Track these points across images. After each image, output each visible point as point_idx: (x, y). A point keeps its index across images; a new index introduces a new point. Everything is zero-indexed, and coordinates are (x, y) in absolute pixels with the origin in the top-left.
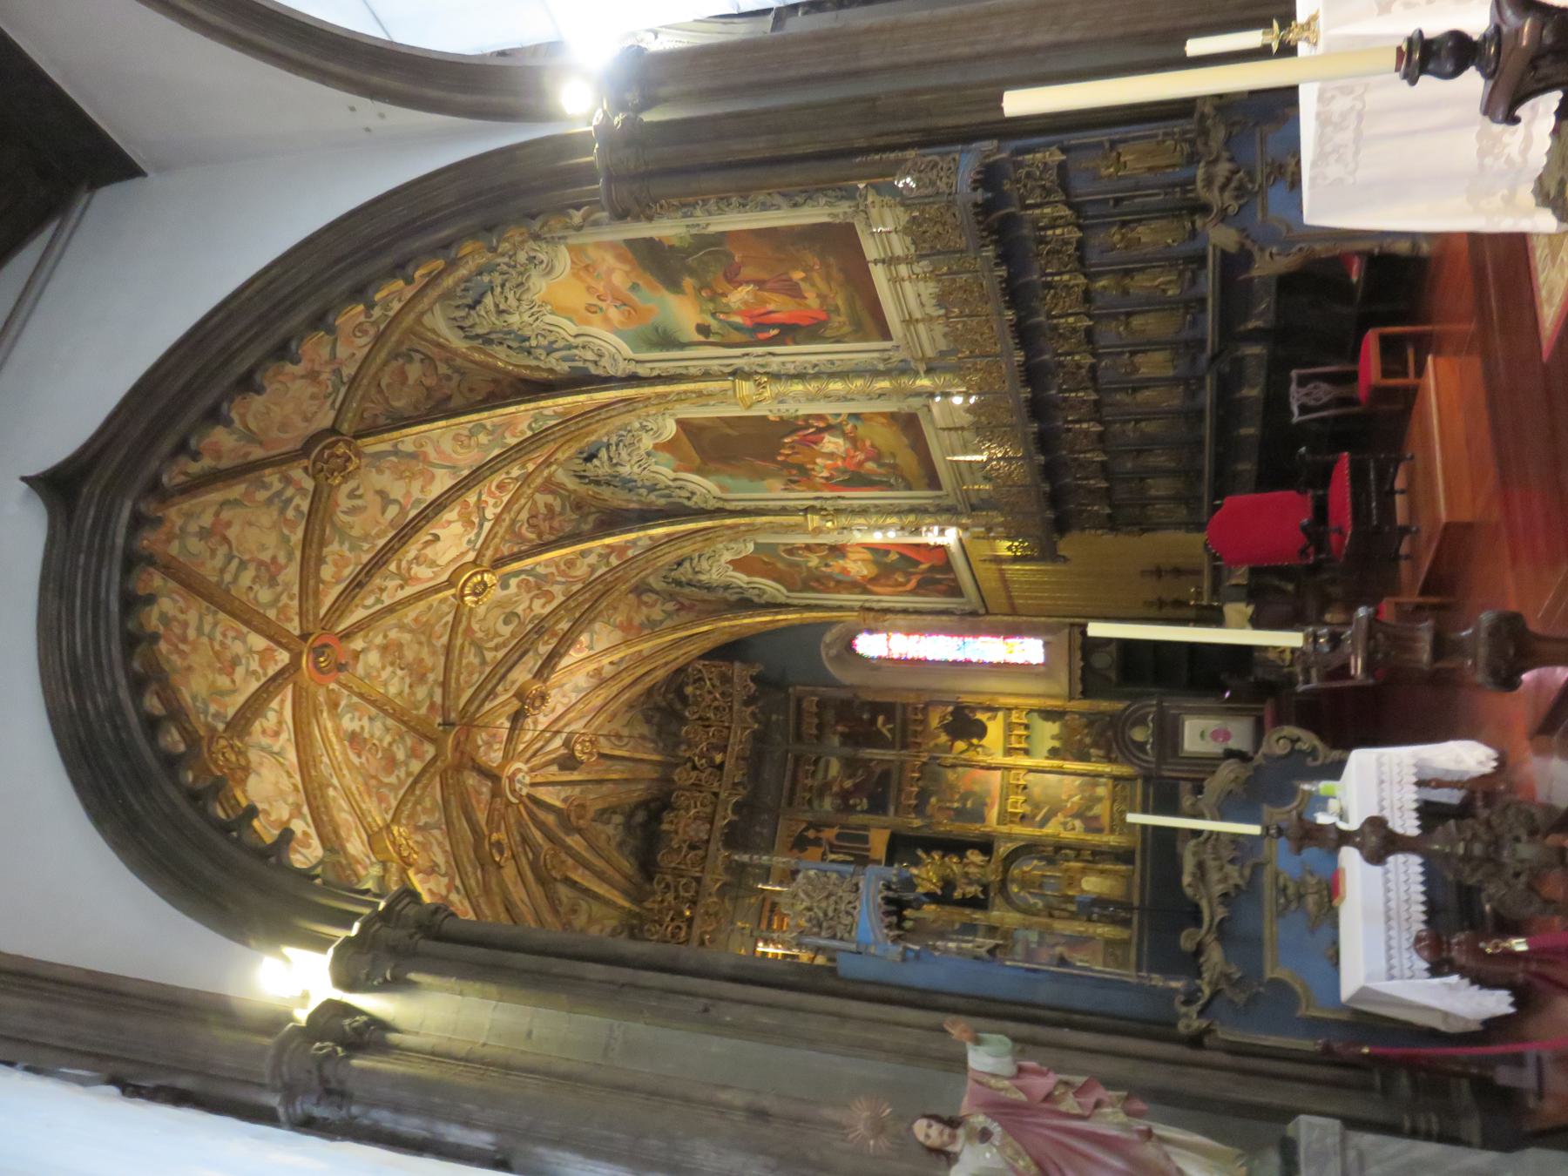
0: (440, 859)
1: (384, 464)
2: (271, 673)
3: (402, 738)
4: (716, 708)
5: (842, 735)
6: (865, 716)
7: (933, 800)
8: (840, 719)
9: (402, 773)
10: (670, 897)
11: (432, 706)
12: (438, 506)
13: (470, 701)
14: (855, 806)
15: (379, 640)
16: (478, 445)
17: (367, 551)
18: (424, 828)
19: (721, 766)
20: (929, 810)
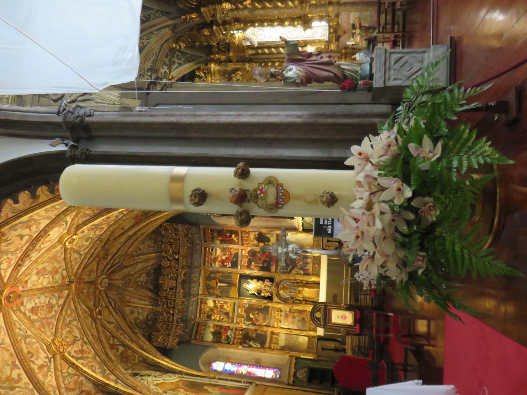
0: (77, 333)
1: (16, 228)
3: (53, 295)
4: (174, 239)
5: (220, 240)
6: (228, 235)
7: (253, 263)
8: (219, 235)
9: (56, 308)
10: (165, 306)
11: (63, 277)
12: (45, 231)
13: (78, 268)
14: (226, 265)
15: (35, 271)
16: (56, 208)
17: (20, 253)
19: (178, 260)
20: (252, 267)
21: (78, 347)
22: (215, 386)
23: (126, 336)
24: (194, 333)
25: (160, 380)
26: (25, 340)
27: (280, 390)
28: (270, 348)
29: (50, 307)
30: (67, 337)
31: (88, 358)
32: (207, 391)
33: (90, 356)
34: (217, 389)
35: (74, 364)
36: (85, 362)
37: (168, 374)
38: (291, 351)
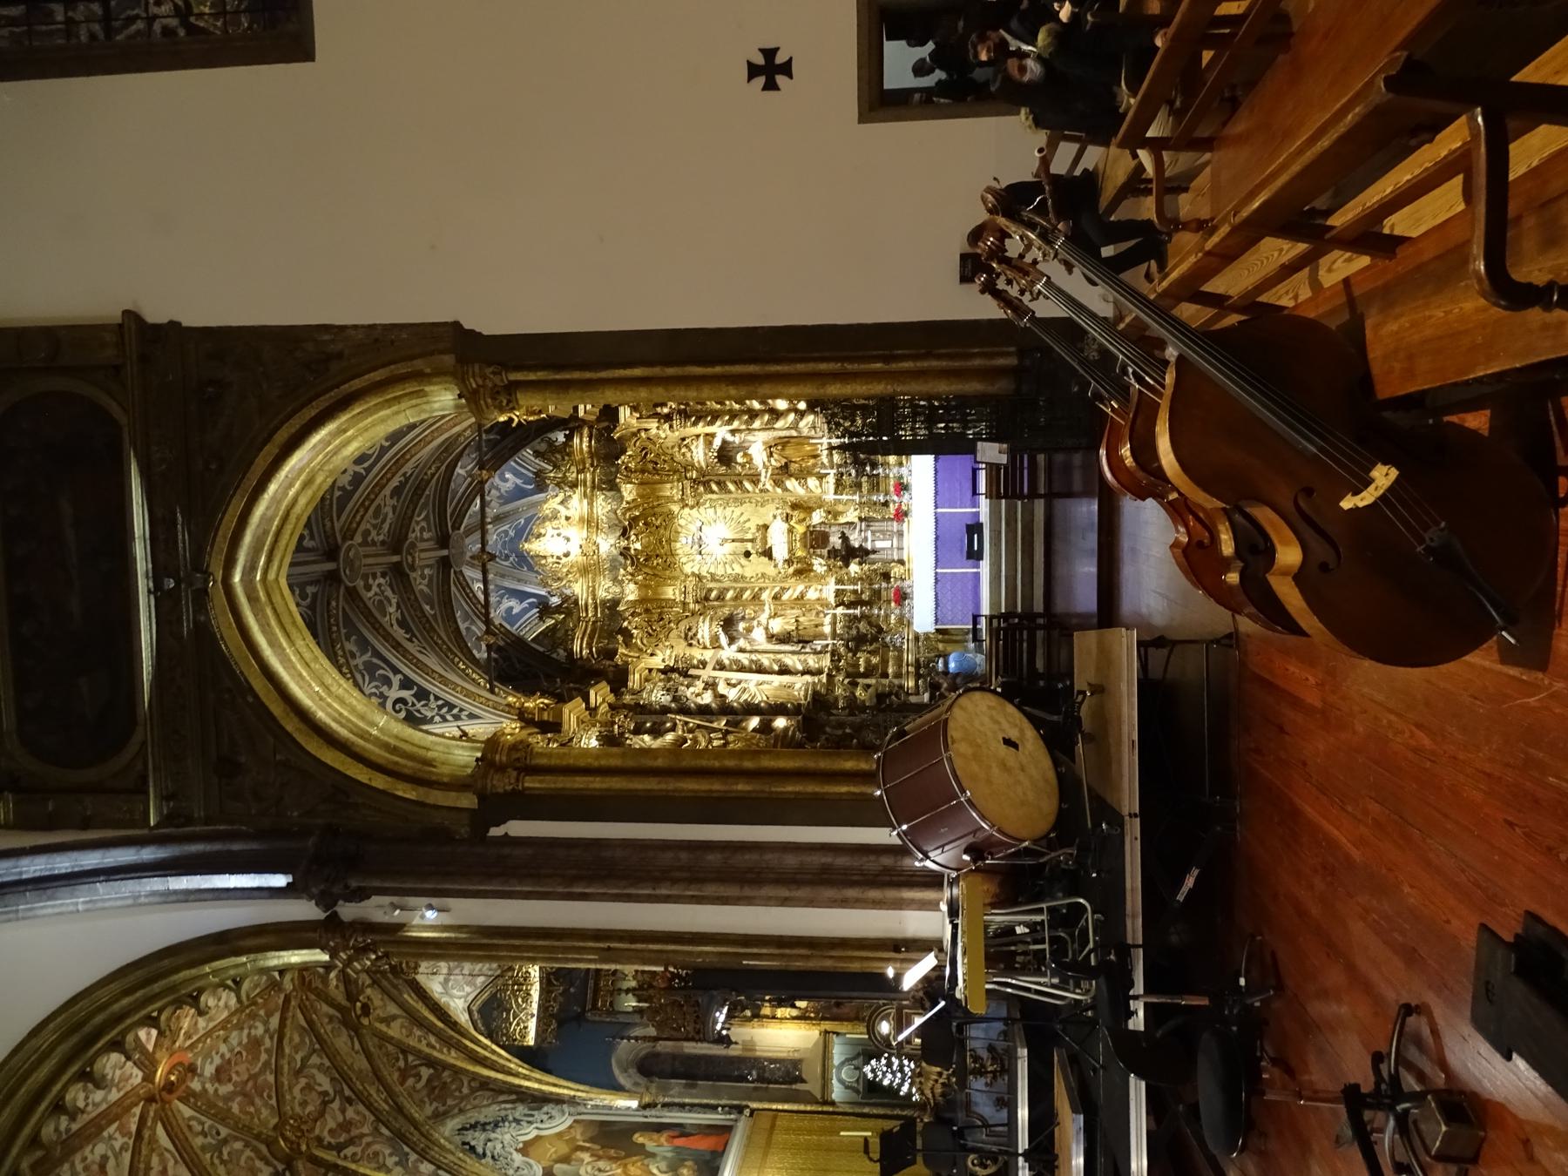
0: (325, 1083)
2: (134, 1128)
9: (268, 1043)
18: (304, 1060)
21: (334, 1118)
22: (659, 1128)
23: (432, 1039)
24: (589, 996)
25: (530, 1133)
26: (221, 1153)
27: (805, 1122)
28: (774, 1017)
29: (255, 1043)
30: (304, 1104)
31: (362, 1136)
32: (641, 1150)
33: (365, 1130)
34: (663, 1140)
35: (336, 1166)
36: (358, 1150)
37: (545, 1109)
38: (824, 1019)
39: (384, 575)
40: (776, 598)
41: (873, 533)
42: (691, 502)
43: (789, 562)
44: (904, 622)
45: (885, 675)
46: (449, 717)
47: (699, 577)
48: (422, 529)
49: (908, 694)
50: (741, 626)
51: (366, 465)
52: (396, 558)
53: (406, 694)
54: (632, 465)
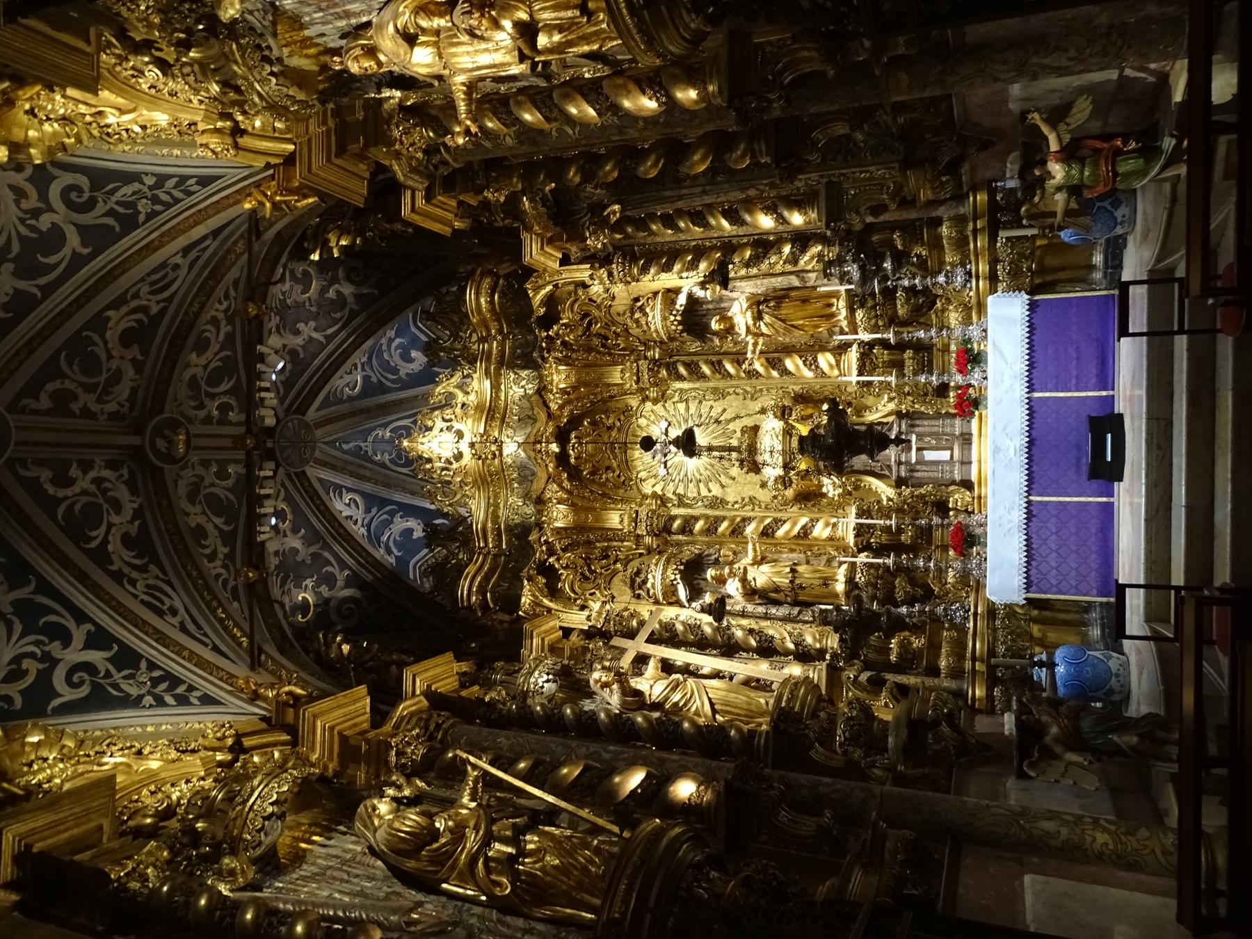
39: (112, 465)
40: (767, 533)
41: (920, 437)
42: (652, 394)
43: (784, 481)
44: (972, 582)
45: (934, 671)
46: (169, 699)
47: (662, 500)
48: (224, 408)
49: (973, 711)
50: (710, 573)
51: (42, 281)
52: (136, 441)
53: (96, 657)
54: (570, 338)
